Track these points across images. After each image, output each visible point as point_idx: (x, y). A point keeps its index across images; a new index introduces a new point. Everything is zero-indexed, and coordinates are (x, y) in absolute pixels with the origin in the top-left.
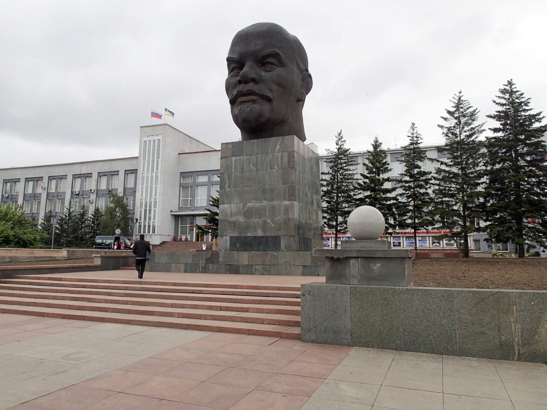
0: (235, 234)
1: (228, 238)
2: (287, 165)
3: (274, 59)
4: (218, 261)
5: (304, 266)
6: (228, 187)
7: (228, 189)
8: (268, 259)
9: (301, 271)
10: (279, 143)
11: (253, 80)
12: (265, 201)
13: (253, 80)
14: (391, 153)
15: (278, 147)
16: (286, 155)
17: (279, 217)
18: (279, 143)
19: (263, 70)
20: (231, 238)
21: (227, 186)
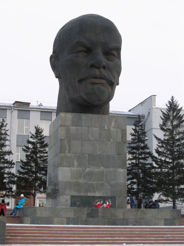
0: (75, 194)
1: (69, 198)
2: (121, 140)
3: (116, 52)
4: (98, 216)
5: (166, 220)
6: (69, 152)
7: (68, 155)
8: (139, 214)
9: (163, 222)
10: (114, 121)
11: (104, 67)
12: (102, 168)
13: (104, 67)
14: (41, 111)
15: (113, 124)
16: (119, 132)
17: (114, 182)
18: (114, 121)
19: (106, 58)
20: (72, 197)
21: (67, 151)
